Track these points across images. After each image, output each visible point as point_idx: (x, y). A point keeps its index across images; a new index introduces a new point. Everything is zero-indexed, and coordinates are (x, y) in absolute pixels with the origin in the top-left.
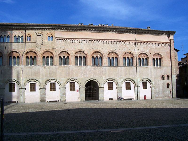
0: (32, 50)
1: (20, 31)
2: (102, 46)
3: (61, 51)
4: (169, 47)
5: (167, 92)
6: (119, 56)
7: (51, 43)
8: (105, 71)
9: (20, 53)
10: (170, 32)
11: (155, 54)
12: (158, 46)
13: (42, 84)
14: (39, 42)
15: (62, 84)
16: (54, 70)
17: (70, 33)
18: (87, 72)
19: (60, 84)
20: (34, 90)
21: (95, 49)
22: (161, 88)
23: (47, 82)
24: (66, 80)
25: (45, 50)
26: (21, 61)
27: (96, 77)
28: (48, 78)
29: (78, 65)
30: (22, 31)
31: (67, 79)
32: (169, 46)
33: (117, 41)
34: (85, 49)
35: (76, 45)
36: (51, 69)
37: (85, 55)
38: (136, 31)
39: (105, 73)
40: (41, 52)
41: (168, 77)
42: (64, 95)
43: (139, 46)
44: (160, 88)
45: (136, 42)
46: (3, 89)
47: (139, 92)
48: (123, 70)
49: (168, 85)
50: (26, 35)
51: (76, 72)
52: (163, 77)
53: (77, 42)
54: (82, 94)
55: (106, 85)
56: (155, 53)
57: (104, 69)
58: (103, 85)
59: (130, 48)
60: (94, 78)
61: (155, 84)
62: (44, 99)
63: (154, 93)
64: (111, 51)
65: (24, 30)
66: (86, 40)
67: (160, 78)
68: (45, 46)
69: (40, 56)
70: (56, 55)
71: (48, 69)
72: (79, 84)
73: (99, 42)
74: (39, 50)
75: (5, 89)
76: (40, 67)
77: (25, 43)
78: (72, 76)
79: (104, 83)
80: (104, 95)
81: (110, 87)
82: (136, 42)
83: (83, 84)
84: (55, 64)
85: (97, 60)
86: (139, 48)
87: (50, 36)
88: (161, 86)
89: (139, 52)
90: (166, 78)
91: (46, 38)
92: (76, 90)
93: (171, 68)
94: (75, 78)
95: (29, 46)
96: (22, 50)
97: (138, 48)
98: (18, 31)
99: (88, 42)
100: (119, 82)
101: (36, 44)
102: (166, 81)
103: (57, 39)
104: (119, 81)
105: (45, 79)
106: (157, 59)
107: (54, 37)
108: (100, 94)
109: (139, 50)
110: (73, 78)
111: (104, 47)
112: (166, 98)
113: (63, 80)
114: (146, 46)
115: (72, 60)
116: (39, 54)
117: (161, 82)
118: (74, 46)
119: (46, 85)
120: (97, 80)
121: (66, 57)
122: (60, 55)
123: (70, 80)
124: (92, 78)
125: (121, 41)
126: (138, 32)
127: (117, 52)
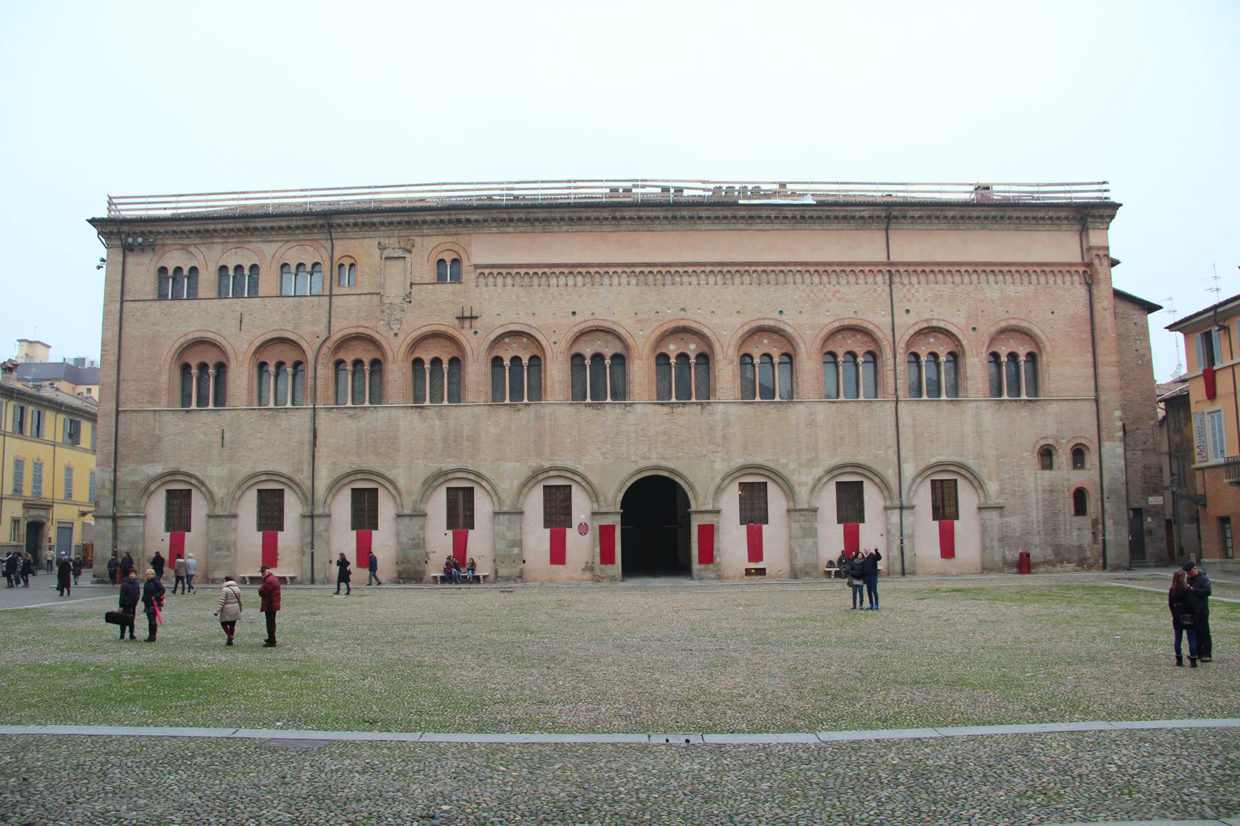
0: (361, 330)
4: (1081, 291)
5: (1075, 534)
6: (802, 345)
7: (453, 293)
9: (304, 345)
10: (1086, 206)
11: (1003, 331)
12: (1020, 289)
14: (394, 290)
15: (503, 496)
17: (547, 238)
19: (493, 493)
21: (672, 316)
22: (1036, 514)
23: (431, 483)
24: (525, 473)
25: (424, 330)
26: (310, 382)
27: (678, 458)
28: (434, 467)
29: (589, 400)
30: (317, 240)
32: (1087, 283)
36: (451, 422)
37: (619, 349)
39: (724, 437)
40: (401, 336)
41: (1078, 455)
42: (516, 550)
43: (909, 291)
44: (1034, 513)
45: (893, 269)
46: (226, 516)
47: (912, 536)
49: (1080, 497)
52: (1046, 455)
53: (580, 283)
56: (1003, 324)
57: (718, 416)
58: (715, 500)
59: (863, 303)
61: (1002, 491)
63: (996, 543)
64: (755, 324)
65: (323, 236)
66: (627, 270)
67: (1033, 460)
69: (401, 356)
71: (437, 423)
73: (694, 280)
74: (395, 327)
75: (235, 516)
76: (400, 413)
77: (331, 296)
78: (553, 454)
79: (719, 490)
82: (893, 269)
84: (470, 396)
85: (685, 370)
86: (909, 300)
87: (448, 257)
88: (1037, 503)
89: (907, 324)
90: (1063, 458)
91: (427, 272)
93: (1097, 401)
94: (570, 464)
95: (351, 314)
97: (901, 301)
99: (633, 281)
100: (800, 484)
101: (382, 303)
102: (1066, 476)
103: (479, 271)
104: (803, 479)
105: (425, 468)
106: (1013, 356)
107: (465, 263)
109: (908, 311)
110: (559, 463)
111: (718, 301)
114: (946, 290)
115: (557, 373)
116: (396, 350)
117: (1039, 481)
120: (685, 473)
121: (525, 361)
122: (577, 349)
123: (545, 475)
124: (654, 461)
125: (812, 269)
126: (904, 217)
127: (789, 329)
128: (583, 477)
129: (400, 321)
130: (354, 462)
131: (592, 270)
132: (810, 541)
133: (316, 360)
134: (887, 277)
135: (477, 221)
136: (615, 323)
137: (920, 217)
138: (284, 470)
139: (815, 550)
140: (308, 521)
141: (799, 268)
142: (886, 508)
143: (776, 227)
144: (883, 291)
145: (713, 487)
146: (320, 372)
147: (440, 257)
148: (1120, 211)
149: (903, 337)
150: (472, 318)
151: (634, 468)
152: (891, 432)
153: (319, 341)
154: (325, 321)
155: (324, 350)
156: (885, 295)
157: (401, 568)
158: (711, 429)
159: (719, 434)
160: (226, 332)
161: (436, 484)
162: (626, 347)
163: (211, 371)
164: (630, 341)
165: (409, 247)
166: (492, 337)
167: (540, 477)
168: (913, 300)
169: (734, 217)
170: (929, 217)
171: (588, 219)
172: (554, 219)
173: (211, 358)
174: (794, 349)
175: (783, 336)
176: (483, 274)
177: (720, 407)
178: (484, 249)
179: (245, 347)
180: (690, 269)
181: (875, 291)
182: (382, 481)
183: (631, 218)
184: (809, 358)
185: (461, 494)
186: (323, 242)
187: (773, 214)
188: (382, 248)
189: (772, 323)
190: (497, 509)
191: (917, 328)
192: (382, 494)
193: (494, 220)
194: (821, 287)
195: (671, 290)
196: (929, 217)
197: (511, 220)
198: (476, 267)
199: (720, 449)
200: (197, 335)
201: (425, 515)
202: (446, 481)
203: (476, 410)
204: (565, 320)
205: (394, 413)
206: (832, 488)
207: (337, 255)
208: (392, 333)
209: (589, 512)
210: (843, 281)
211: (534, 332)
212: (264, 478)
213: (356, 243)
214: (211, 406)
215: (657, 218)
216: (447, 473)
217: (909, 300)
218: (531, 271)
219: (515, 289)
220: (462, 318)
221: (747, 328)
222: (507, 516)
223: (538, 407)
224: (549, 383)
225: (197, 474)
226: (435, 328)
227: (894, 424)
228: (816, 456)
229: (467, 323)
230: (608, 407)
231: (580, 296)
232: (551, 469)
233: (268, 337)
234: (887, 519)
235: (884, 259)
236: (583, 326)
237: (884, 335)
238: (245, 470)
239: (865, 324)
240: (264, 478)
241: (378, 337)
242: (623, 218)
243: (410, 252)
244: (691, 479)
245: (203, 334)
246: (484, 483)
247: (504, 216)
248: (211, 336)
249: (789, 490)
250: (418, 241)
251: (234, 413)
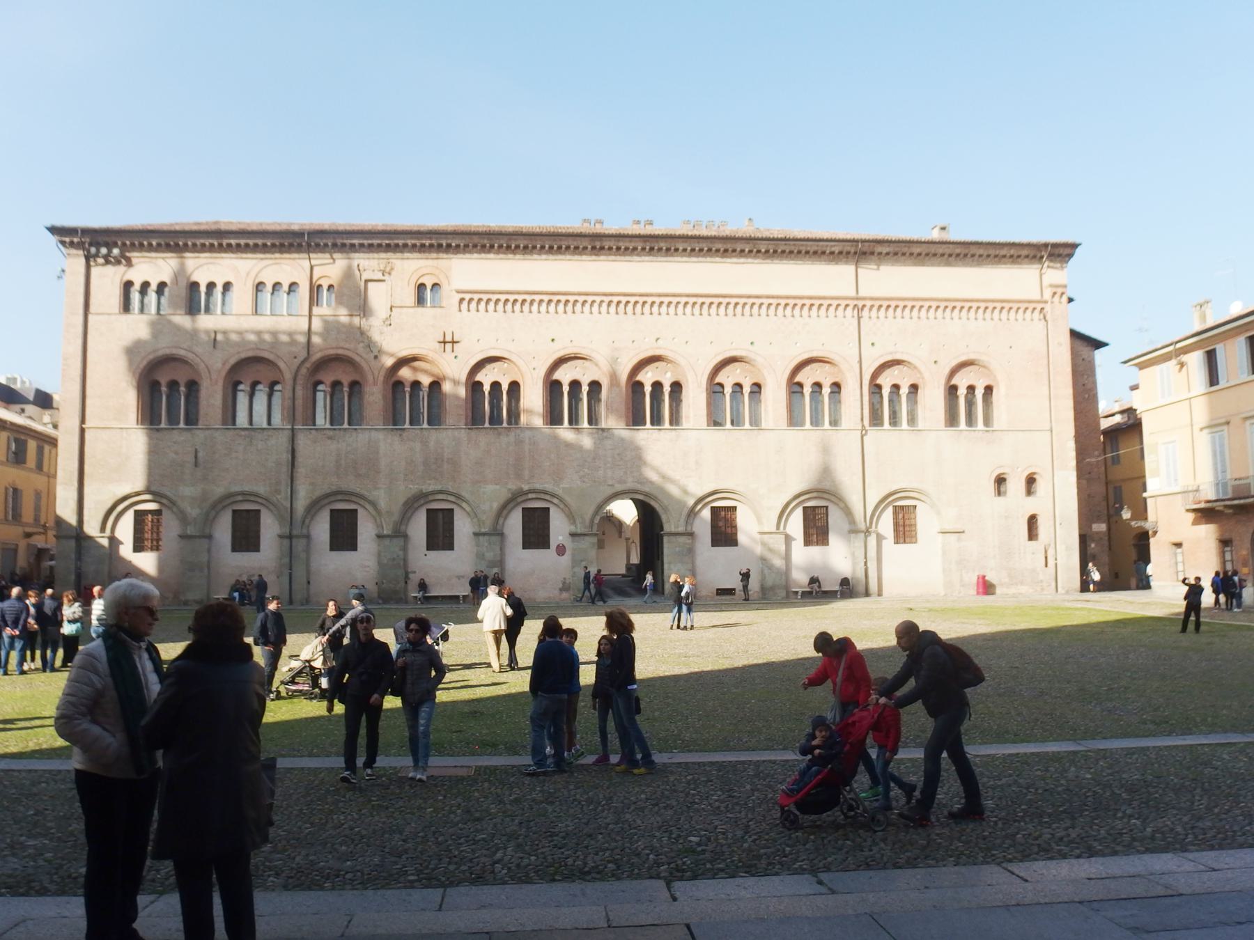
0: (340, 352)
9: (282, 365)
13: (389, 513)
24: (504, 495)
28: (414, 488)
36: (432, 444)
38: (861, 251)
41: (1031, 481)
49: (1032, 521)
52: (1000, 481)
69: (381, 378)
87: (429, 283)
90: (1016, 485)
92: (554, 543)
94: (549, 487)
105: (405, 490)
110: (538, 486)
112: (1024, 589)
113: (491, 495)
116: (376, 373)
128: (561, 500)
130: (332, 483)
137: (888, 254)
138: (261, 489)
140: (286, 542)
148: (1078, 250)
150: (453, 342)
153: (297, 362)
160: (199, 350)
163: (182, 389)
167: (519, 500)
173: (182, 378)
179: (219, 365)
185: (440, 515)
192: (361, 514)
200: (168, 351)
203: (456, 433)
205: (374, 434)
212: (240, 498)
214: (182, 425)
222: (486, 538)
223: (518, 431)
225: (168, 494)
232: (531, 491)
233: (243, 355)
238: (219, 491)
240: (240, 498)
241: (358, 359)
245: (174, 351)
248: (182, 353)
251: (207, 432)
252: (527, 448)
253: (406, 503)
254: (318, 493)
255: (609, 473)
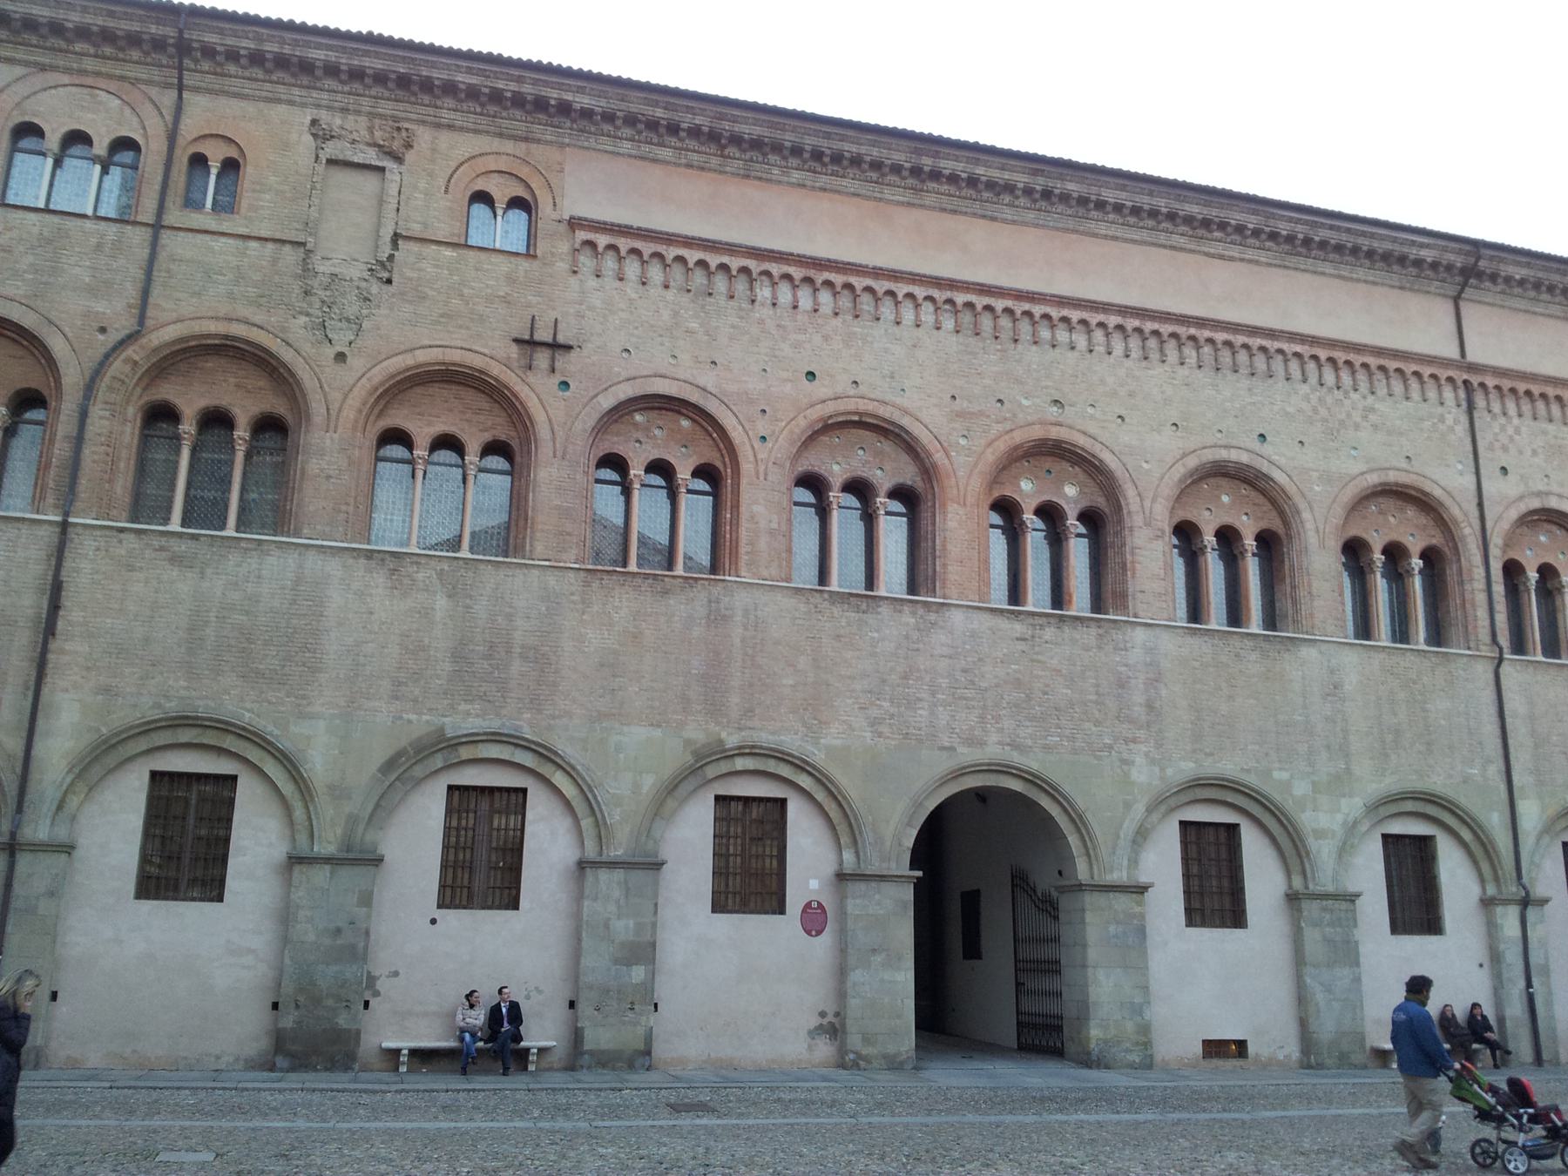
0: (238, 330)
1: (102, 83)
2: (1110, 380)
3: (626, 391)
6: (1306, 515)
7: (511, 279)
8: (1156, 680)
9: (57, 346)
13: (338, 792)
14: (345, 244)
15: (614, 816)
16: (519, 622)
17: (752, 192)
18: (944, 682)
19: (585, 807)
20: (212, 887)
21: (1033, 415)
23: (403, 769)
24: (675, 757)
25: (422, 356)
28: (420, 723)
30: (135, 82)
31: (688, 742)
33: (1277, 345)
34: (922, 406)
35: (817, 339)
37: (907, 474)
39: (1150, 706)
40: (356, 363)
42: (638, 973)
43: (1503, 428)
45: (1475, 380)
48: (1351, 681)
50: (181, 142)
51: (803, 662)
54: (878, 958)
55: (1163, 866)
57: (1136, 655)
58: (1134, 862)
60: (1017, 759)
62: (343, 1021)
65: (156, 75)
66: (936, 293)
68: (424, 298)
69: (349, 414)
70: (560, 434)
71: (441, 603)
72: (842, 821)
76: (334, 567)
77: (157, 227)
78: (749, 712)
79: (1142, 835)
80: (1145, 989)
81: (1215, 896)
83: (888, 832)
86: (1505, 449)
87: (502, 191)
89: (1508, 497)
92: (795, 899)
94: (792, 742)
95: (213, 280)
96: (100, 307)
98: (68, 71)
100: (1320, 834)
101: (307, 270)
103: (582, 235)
105: (390, 723)
107: (545, 209)
108: (1101, 974)
109: (1504, 470)
110: (765, 738)
111: (1131, 395)
113: (631, 755)
116: (336, 396)
118: (797, 346)
119: (382, 808)
120: (1067, 788)
123: (724, 767)
124: (993, 750)
125: (1323, 354)
129: (357, 324)
130: (176, 691)
131: (859, 282)
132: (1343, 974)
133: (89, 389)
134: (1462, 394)
135: (587, 114)
136: (906, 412)
139: (1353, 1002)
141: (1298, 348)
142: (1487, 903)
143: (1250, 254)
144: (1456, 422)
145: (1129, 827)
146: (99, 420)
147: (480, 185)
149: (1501, 521)
150: (556, 346)
151: (945, 764)
152: (1490, 728)
153: (106, 341)
154: (131, 292)
155: (118, 367)
156: (1462, 429)
157: (288, 1021)
158: (1122, 684)
159: (1138, 698)
161: (418, 771)
162: (928, 470)
164: (939, 457)
165: (396, 145)
166: (607, 402)
167: (711, 771)
168: (1513, 451)
169: (1172, 217)
170: (1537, 286)
171: (856, 161)
172: (777, 148)
174: (1286, 523)
175: (1263, 492)
176: (591, 244)
177: (1140, 635)
178: (594, 185)
180: (1075, 315)
181: (1442, 419)
182: (254, 754)
183: (953, 179)
184: (1322, 545)
186: (154, 92)
187: (1252, 221)
188: (321, 134)
189: (1244, 458)
190: (591, 851)
191: (1523, 507)
192: (248, 794)
193: (631, 120)
194: (1338, 394)
195: (1033, 355)
196: (1537, 286)
197: (674, 129)
198: (574, 224)
199: (1141, 734)
201: (378, 861)
202: (448, 767)
203: (552, 580)
204: (788, 388)
205: (313, 562)
206: (1375, 848)
207: (191, 125)
208: (330, 352)
209: (829, 868)
210: (1382, 390)
211: (712, 407)
213: (250, 108)
215: (1010, 188)
216: (455, 744)
217: (1505, 449)
218: (714, 260)
219: (670, 295)
220: (529, 344)
221: (1192, 462)
222: (619, 874)
223: (717, 590)
224: (744, 534)
226: (456, 356)
227: (1492, 710)
228: (1348, 770)
229: (542, 358)
230: (885, 610)
231: (826, 338)
234: (1492, 928)
235: (1452, 352)
236: (830, 408)
237: (1462, 511)
239: (1428, 487)
241: (287, 355)
242: (936, 175)
243: (399, 159)
244: (1080, 802)
246: (559, 779)
247: (659, 113)
249: (1291, 847)
250: (424, 136)
252: (737, 633)
253: (390, 765)
254: (123, 716)
255: (943, 716)
